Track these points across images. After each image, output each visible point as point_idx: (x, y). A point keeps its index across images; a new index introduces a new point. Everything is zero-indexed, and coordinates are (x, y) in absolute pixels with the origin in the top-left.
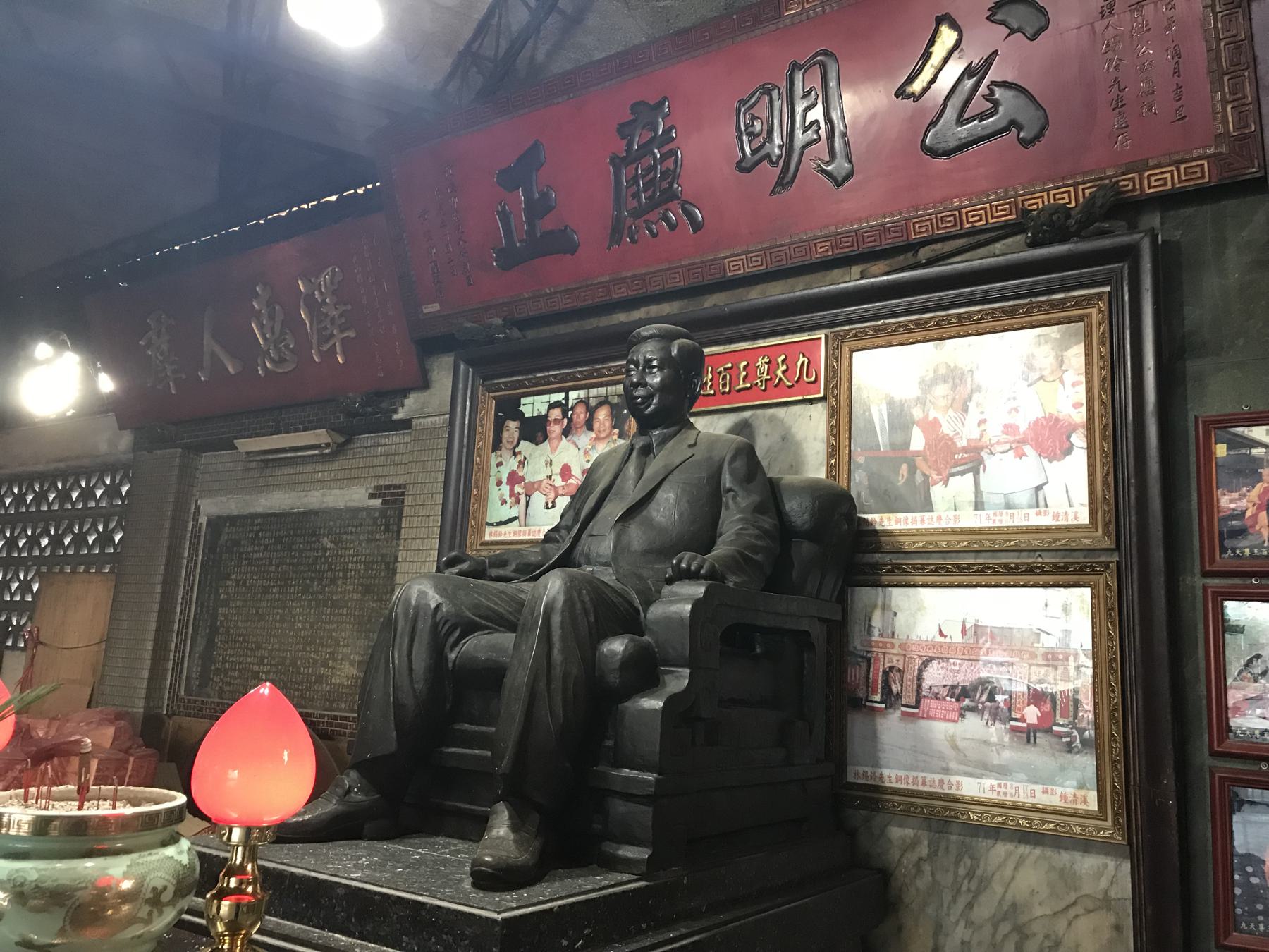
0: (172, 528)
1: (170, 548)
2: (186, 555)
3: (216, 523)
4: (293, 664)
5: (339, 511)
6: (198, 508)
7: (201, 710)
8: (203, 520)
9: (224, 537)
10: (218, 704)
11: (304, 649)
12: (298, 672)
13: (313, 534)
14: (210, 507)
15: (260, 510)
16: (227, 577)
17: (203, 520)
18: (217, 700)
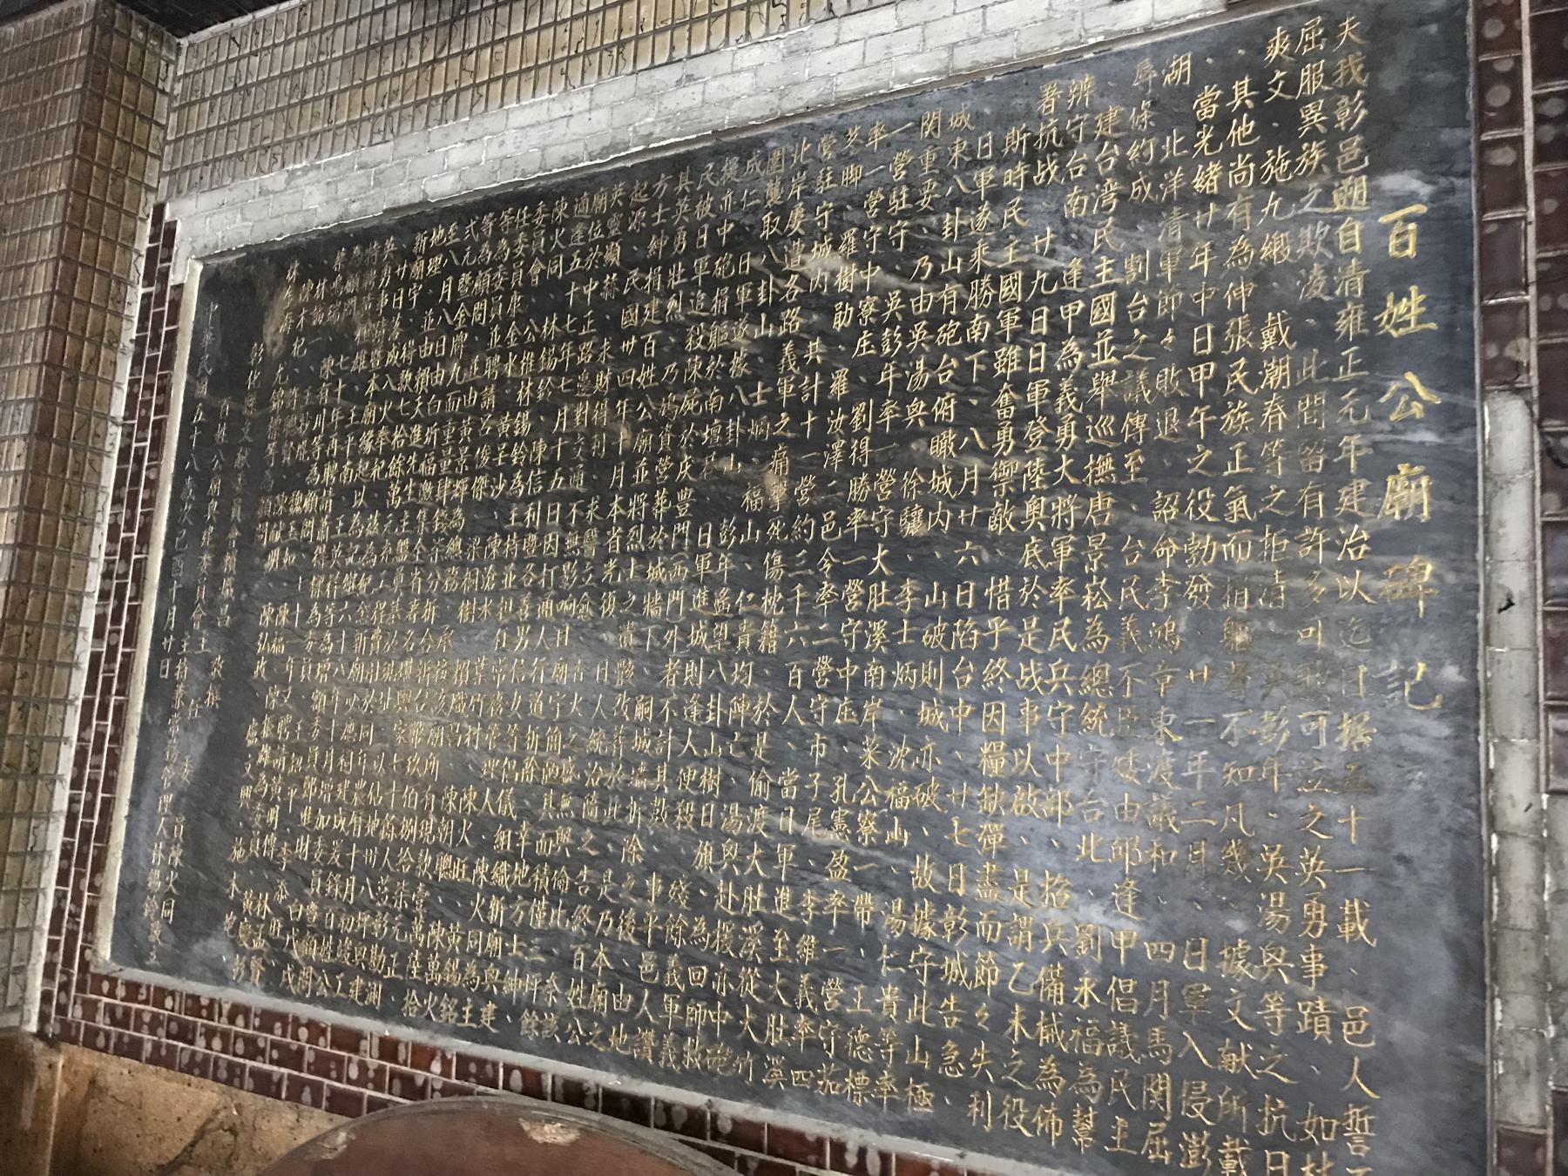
0: (62, 294)
1: (53, 365)
2: (118, 408)
3: (240, 283)
4: (668, 859)
5: (903, 107)
6: (165, 235)
7: (185, 1033)
8: (187, 273)
9: (276, 327)
10: (269, 1019)
11: (731, 791)
12: (701, 905)
13: (744, 239)
14: (212, 221)
15: (442, 187)
16: (294, 478)
17: (187, 273)
18: (258, 999)
